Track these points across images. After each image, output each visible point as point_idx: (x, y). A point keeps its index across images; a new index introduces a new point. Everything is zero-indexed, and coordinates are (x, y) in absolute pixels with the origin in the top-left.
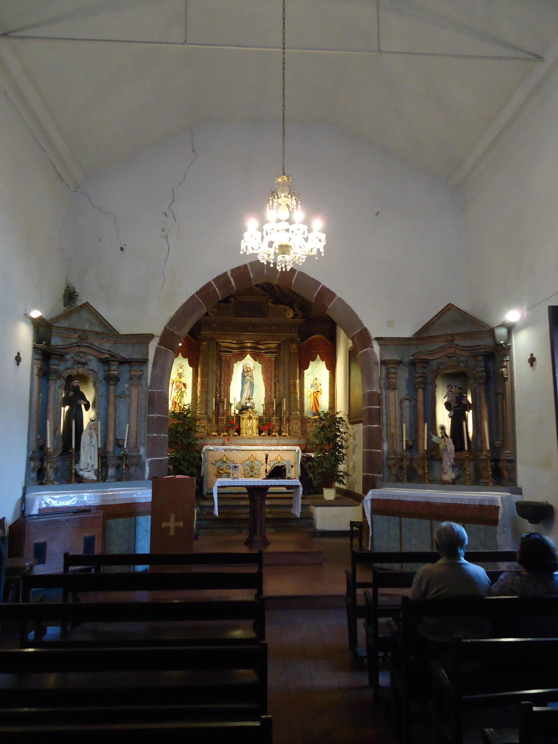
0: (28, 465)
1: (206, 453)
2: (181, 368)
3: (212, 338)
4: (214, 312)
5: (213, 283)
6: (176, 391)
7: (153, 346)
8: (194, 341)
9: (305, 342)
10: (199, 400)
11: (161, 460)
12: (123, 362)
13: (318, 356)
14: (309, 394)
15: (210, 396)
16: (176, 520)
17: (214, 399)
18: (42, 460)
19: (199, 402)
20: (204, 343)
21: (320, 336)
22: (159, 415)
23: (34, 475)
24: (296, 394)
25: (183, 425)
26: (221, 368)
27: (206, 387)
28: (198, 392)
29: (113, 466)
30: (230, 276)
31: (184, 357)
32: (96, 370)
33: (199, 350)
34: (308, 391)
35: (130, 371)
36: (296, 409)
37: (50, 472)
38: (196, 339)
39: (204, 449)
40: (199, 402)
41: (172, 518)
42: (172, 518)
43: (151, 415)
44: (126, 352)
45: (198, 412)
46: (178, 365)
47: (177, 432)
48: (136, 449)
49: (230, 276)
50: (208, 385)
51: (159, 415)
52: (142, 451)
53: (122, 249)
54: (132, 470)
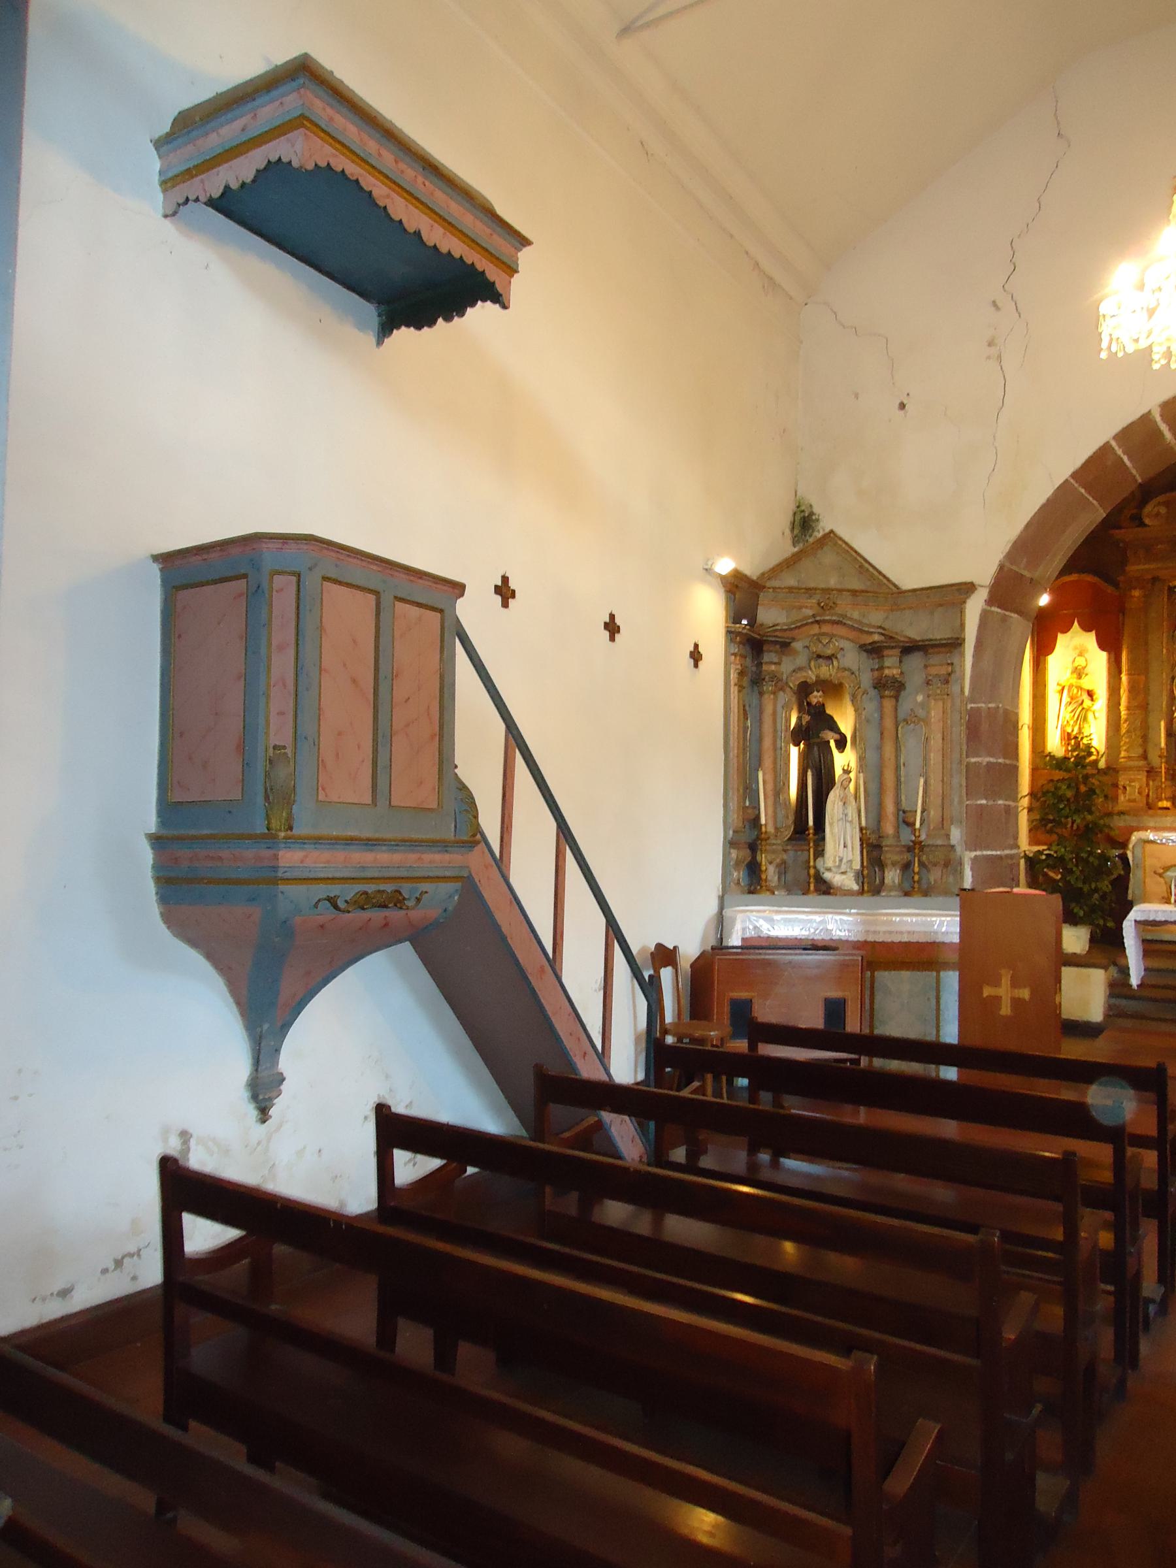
0: (726, 855)
1: (1138, 851)
2: (1081, 655)
3: (1155, 579)
4: (1158, 514)
5: (1114, 444)
6: (1070, 708)
7: (974, 607)
8: (1110, 589)
10: (1124, 727)
11: (1000, 857)
12: (910, 648)
15: (1152, 719)
16: (1015, 984)
17: (1162, 724)
18: (753, 847)
19: (1123, 731)
20: (1136, 593)
22: (992, 760)
23: (739, 875)
25: (1072, 783)
28: (1122, 708)
29: (894, 864)
30: (1158, 419)
31: (1086, 628)
32: (855, 668)
33: (1122, 610)
35: (926, 666)
37: (770, 873)
38: (1116, 585)
39: (1135, 837)
40: (1123, 731)
41: (1006, 981)
42: (1006, 981)
43: (973, 760)
44: (914, 628)
45: (1123, 754)
46: (1075, 648)
47: (1061, 799)
48: (943, 832)
49: (1158, 419)
50: (1147, 690)
51: (992, 760)
52: (956, 835)
53: (902, 406)
54: (935, 875)
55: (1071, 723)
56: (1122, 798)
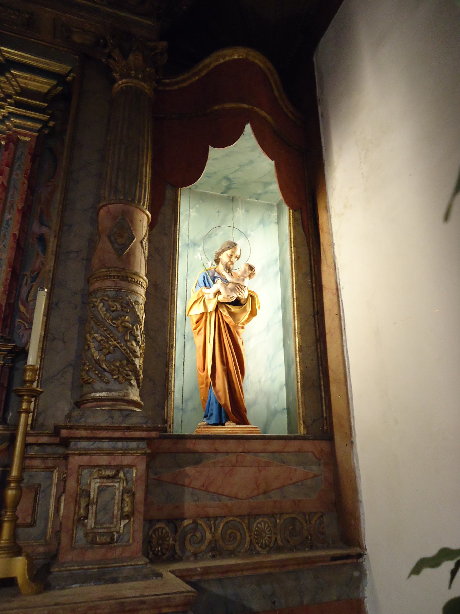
9: (187, 79)
13: (248, 128)
14: (198, 309)
21: (257, 59)
24: (129, 277)
34: (193, 296)
36: (123, 368)
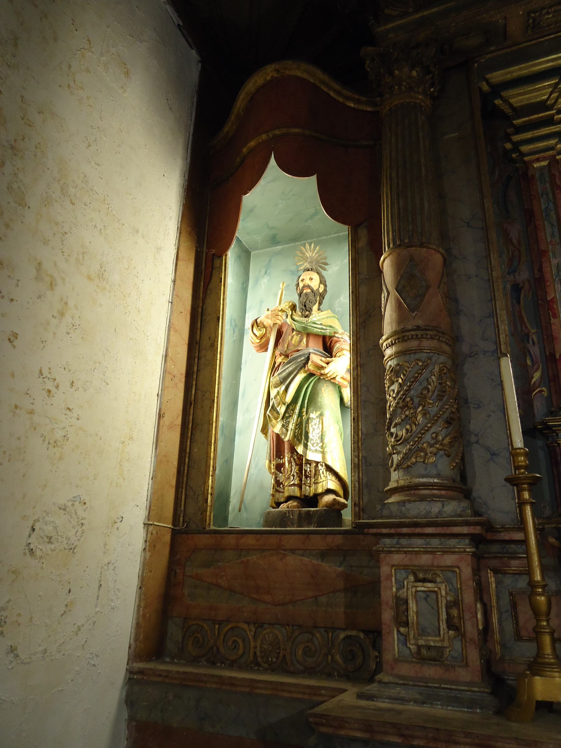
17: (507, 367)
19: (391, 401)
26: (529, 215)
27: (435, 302)
31: (294, 167)
40: (391, 401)
45: (396, 478)
55: (282, 409)
56: (393, 643)
